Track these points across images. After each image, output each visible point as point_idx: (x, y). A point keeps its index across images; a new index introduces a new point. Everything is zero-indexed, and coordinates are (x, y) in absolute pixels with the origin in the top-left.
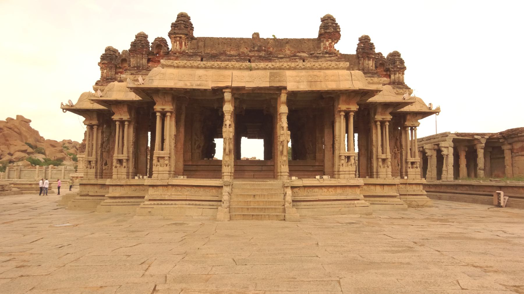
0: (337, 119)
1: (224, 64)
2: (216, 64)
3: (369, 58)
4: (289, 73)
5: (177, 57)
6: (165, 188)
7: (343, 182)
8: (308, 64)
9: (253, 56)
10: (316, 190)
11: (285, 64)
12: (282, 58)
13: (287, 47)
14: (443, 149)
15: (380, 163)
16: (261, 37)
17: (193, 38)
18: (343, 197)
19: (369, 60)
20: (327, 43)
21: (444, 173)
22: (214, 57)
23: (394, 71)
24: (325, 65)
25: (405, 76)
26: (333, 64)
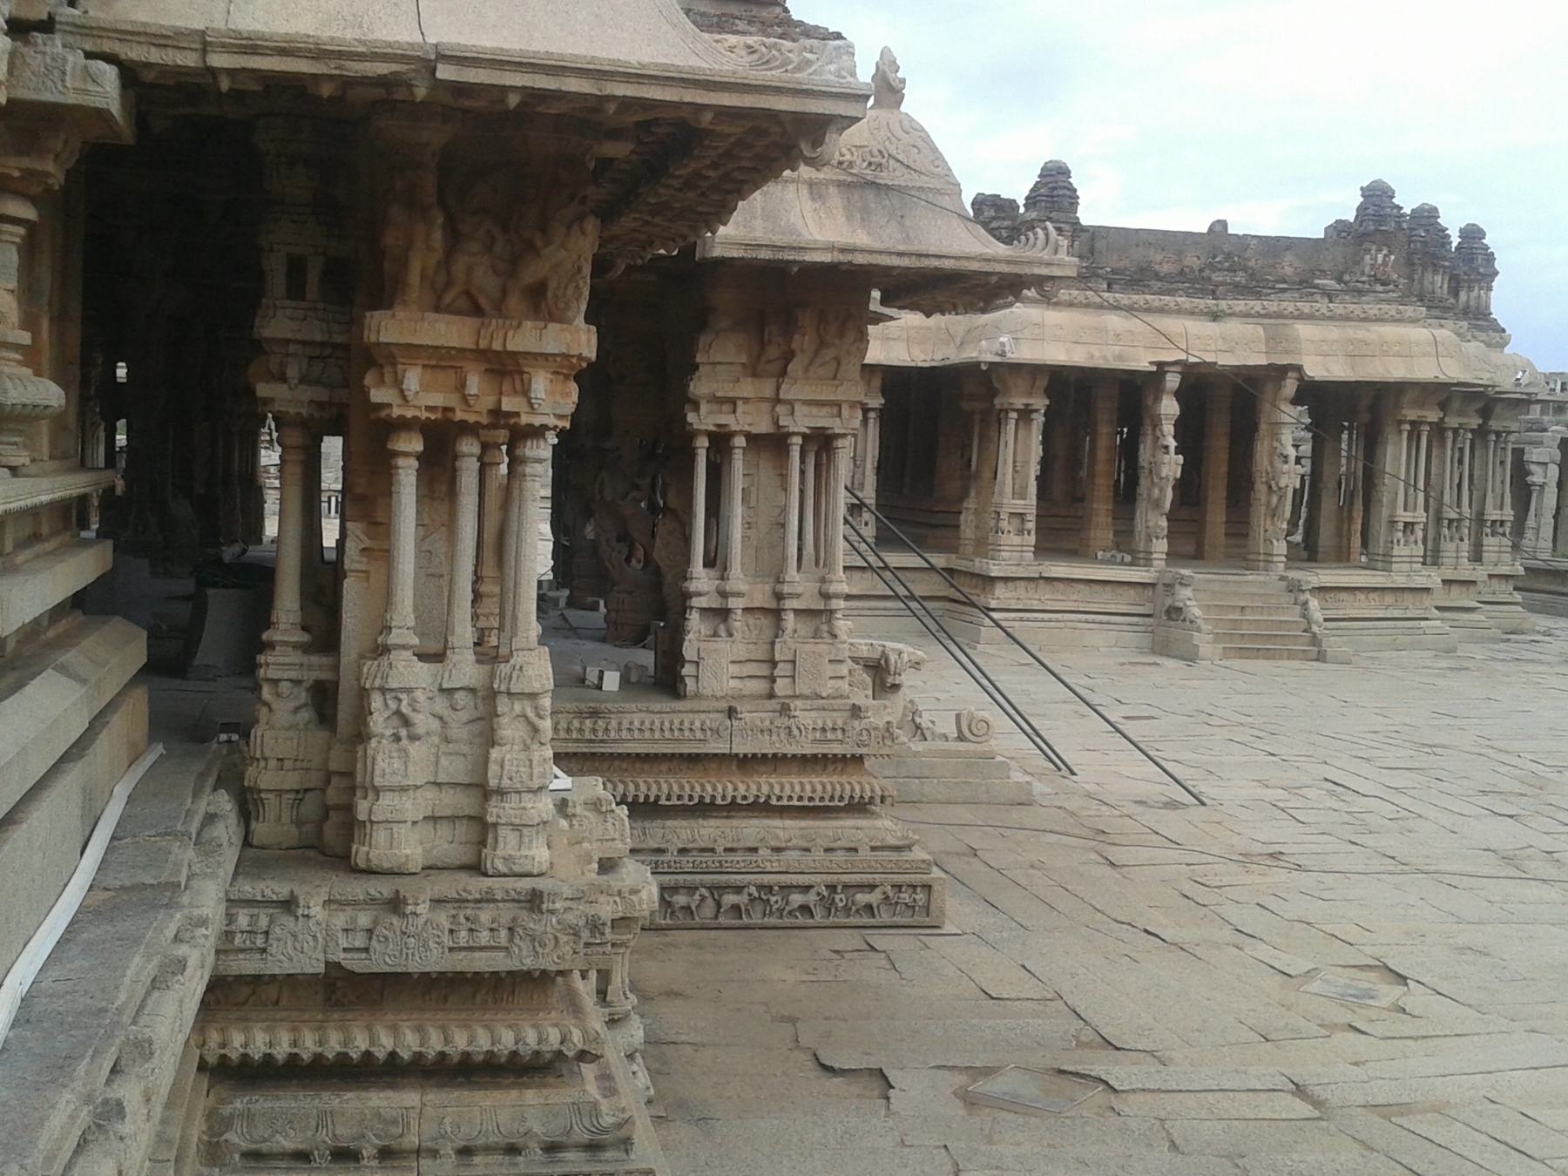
0: (1391, 438)
4: (1304, 330)
6: (1032, 585)
7: (1400, 581)
8: (1337, 308)
9: (1223, 284)
10: (1343, 596)
11: (1290, 307)
12: (1283, 290)
13: (1289, 257)
14: (1533, 468)
16: (1230, 231)
18: (1397, 614)
19: (1435, 272)
20: (1380, 257)
21: (1529, 534)
23: (1470, 281)
24: (1373, 310)
26: (1391, 310)
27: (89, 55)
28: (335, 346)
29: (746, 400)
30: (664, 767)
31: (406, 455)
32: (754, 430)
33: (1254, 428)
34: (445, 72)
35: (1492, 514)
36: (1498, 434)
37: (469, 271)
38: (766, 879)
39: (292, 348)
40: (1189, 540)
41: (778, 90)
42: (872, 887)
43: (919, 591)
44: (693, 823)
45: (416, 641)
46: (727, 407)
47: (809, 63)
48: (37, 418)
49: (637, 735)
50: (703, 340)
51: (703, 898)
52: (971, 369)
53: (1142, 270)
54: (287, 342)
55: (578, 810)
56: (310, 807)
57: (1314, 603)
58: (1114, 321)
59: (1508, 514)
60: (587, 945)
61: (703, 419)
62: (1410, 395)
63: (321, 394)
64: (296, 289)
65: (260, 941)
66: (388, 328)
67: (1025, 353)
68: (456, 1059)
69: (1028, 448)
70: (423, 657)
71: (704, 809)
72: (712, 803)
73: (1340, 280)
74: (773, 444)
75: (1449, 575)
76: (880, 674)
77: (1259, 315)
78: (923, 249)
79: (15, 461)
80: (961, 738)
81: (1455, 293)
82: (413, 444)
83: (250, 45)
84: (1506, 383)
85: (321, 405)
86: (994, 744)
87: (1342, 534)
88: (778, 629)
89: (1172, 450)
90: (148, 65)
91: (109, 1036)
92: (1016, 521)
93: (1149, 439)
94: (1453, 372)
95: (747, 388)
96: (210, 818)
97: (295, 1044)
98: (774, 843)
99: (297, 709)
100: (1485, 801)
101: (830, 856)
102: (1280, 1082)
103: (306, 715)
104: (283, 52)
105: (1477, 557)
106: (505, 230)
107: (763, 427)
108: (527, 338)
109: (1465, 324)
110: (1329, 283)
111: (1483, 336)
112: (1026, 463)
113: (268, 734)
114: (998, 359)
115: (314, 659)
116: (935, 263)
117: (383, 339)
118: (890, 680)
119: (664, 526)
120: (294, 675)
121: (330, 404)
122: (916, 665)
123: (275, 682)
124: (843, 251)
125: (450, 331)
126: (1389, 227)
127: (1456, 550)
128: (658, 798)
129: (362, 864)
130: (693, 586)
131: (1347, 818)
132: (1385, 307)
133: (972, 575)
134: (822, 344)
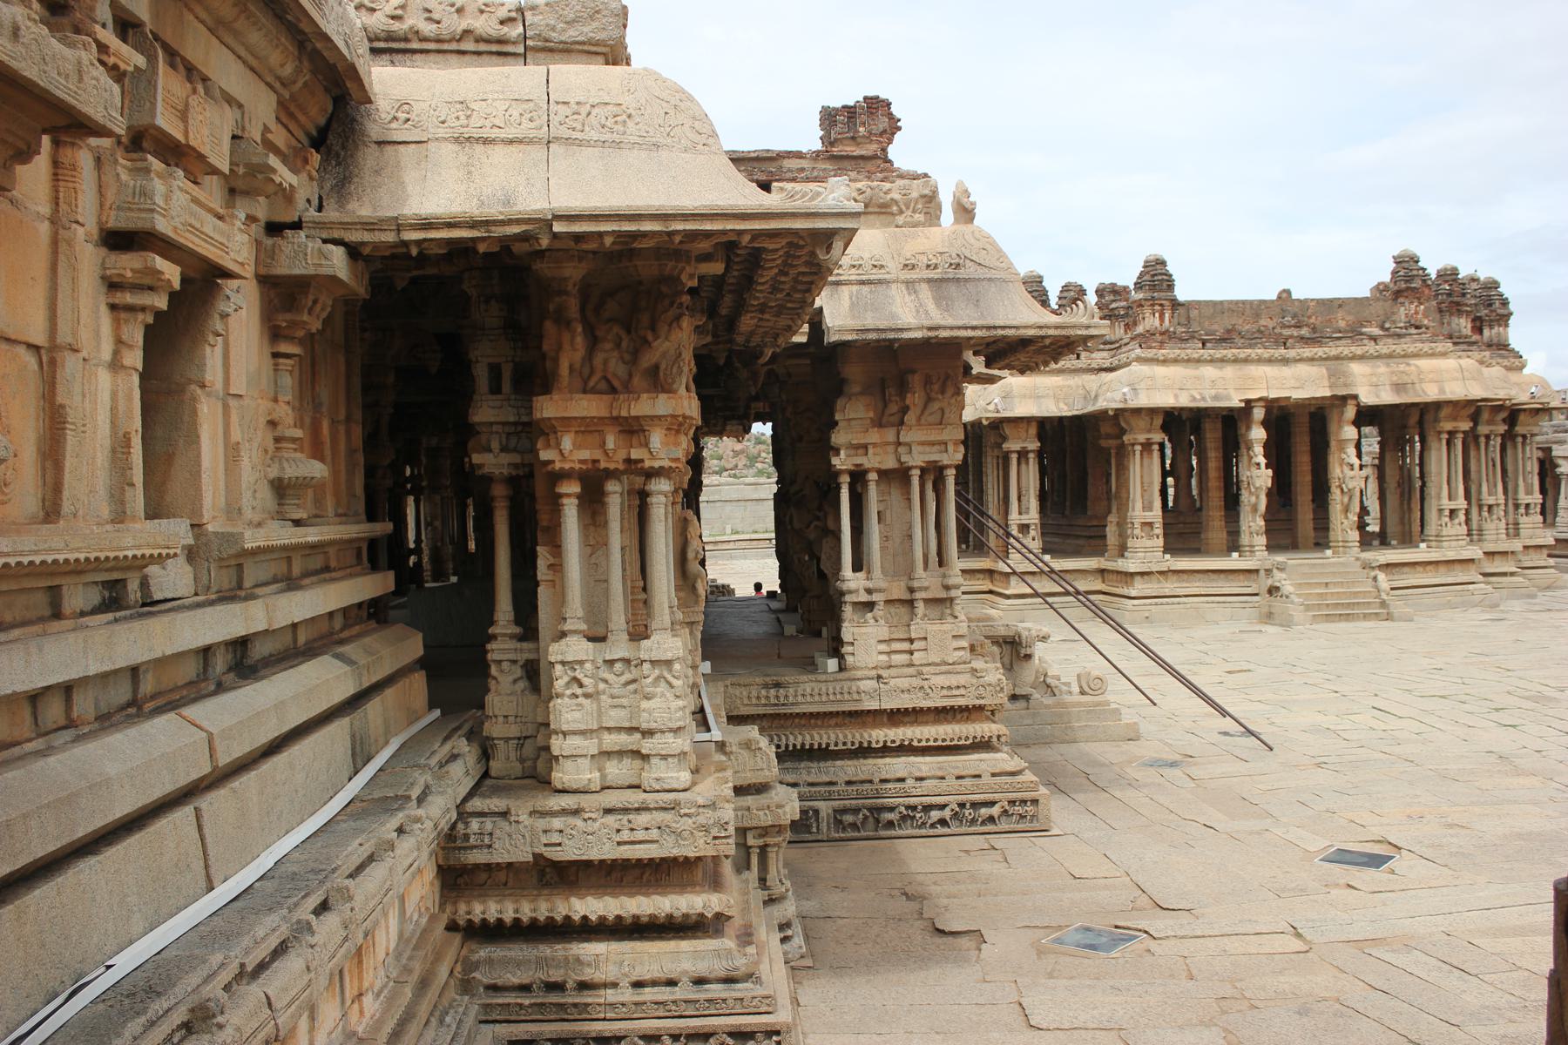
1: (1243, 353)
2: (1229, 353)
3: (1460, 313)
4: (1356, 368)
5: (1162, 342)
7: (1451, 555)
9: (1291, 337)
10: (1406, 569)
11: (1346, 352)
14: (1560, 462)
15: (1485, 514)
16: (1294, 296)
17: (1175, 304)
18: (1450, 580)
22: (1225, 340)
24: (1412, 348)
25: (1510, 330)
26: (1426, 347)
27: (325, 241)
28: (524, 424)
29: (875, 445)
30: (833, 722)
31: (568, 495)
32: (884, 467)
33: (1327, 445)
34: (558, 227)
35: (1524, 498)
36: (1524, 437)
37: (606, 362)
38: (913, 801)
39: (495, 428)
40: (1282, 534)
41: (794, 215)
42: (992, 804)
43: (1082, 588)
44: (855, 762)
45: (584, 627)
46: (861, 451)
47: (819, 194)
48: (307, 486)
49: (809, 699)
50: (840, 403)
51: (866, 818)
52: (1103, 414)
53: (1229, 331)
54: (491, 424)
55: (734, 749)
56: (529, 749)
57: (1381, 576)
58: (1209, 371)
59: (1537, 498)
60: (715, 838)
61: (841, 462)
62: (1444, 412)
63: (516, 458)
64: (496, 389)
65: (487, 841)
66: (547, 408)
67: (1143, 401)
68: (629, 921)
69: (1151, 471)
70: (591, 639)
71: (864, 751)
72: (869, 747)
73: (1382, 328)
74: (898, 477)
75: (1491, 547)
76: (1014, 649)
77: (1321, 359)
78: (990, 322)
79: (296, 516)
80: (1083, 693)
81: (1480, 331)
82: (572, 488)
83: (427, 224)
84: (1521, 397)
85: (516, 466)
86: (1109, 697)
87: (1404, 521)
88: (913, 614)
89: (1263, 466)
90: (363, 244)
91: (322, 882)
92: (1147, 528)
93: (1245, 458)
94: (1476, 392)
95: (874, 436)
96: (454, 757)
97: (517, 911)
98: (918, 774)
99: (515, 681)
100: (1495, 716)
101: (960, 782)
102: (1283, 926)
103: (521, 685)
104: (450, 225)
105: (1514, 530)
106: (629, 332)
107: (890, 463)
108: (645, 406)
109: (1487, 353)
110: (1376, 331)
111: (1506, 362)
112: (1151, 483)
113: (496, 699)
114: (1121, 406)
115: (525, 645)
116: (1000, 332)
117: (545, 415)
118: (1023, 652)
119: (827, 544)
120: (512, 656)
121: (524, 465)
122: (1044, 639)
123: (499, 662)
124: (930, 329)
125: (588, 406)
126: (1416, 284)
127: (1495, 528)
128: (828, 745)
129: (560, 787)
130: (845, 587)
131: (1383, 735)
132: (1419, 345)
133: (1118, 572)
134: (929, 400)
